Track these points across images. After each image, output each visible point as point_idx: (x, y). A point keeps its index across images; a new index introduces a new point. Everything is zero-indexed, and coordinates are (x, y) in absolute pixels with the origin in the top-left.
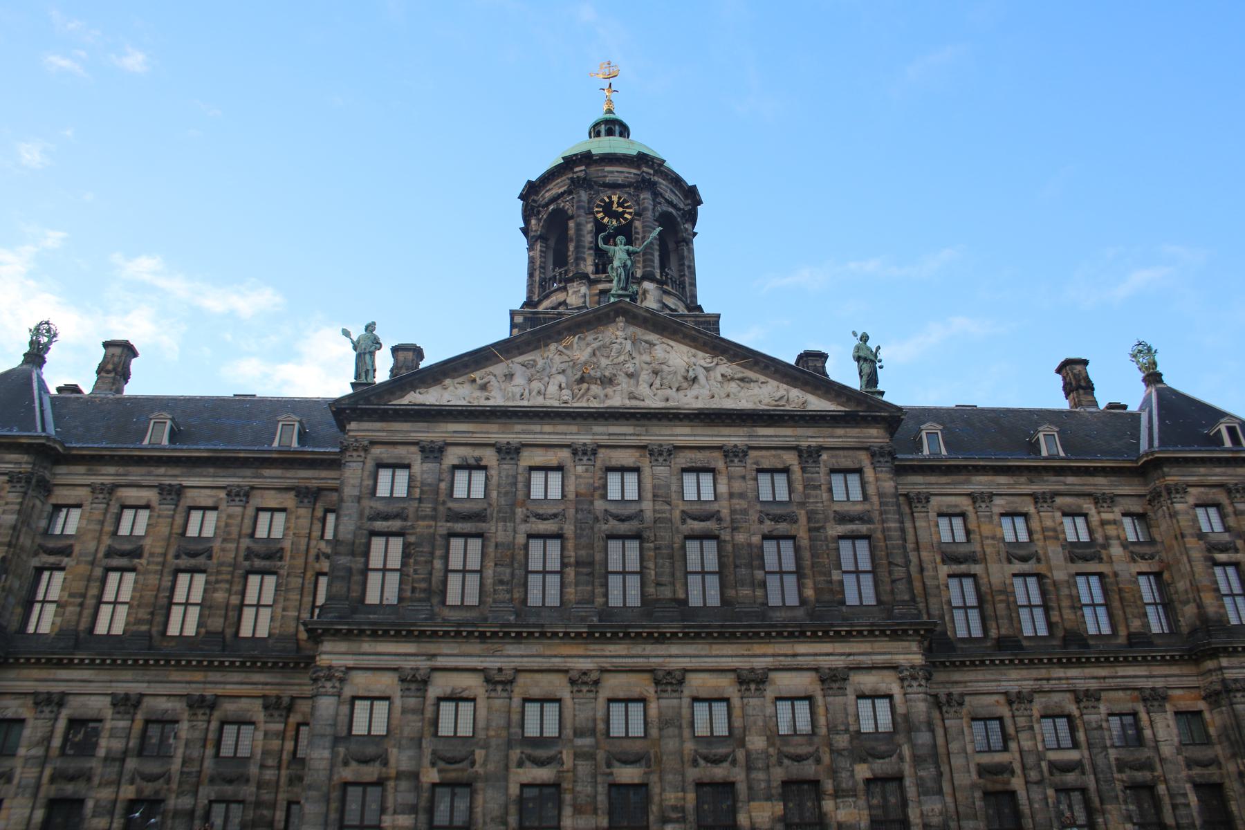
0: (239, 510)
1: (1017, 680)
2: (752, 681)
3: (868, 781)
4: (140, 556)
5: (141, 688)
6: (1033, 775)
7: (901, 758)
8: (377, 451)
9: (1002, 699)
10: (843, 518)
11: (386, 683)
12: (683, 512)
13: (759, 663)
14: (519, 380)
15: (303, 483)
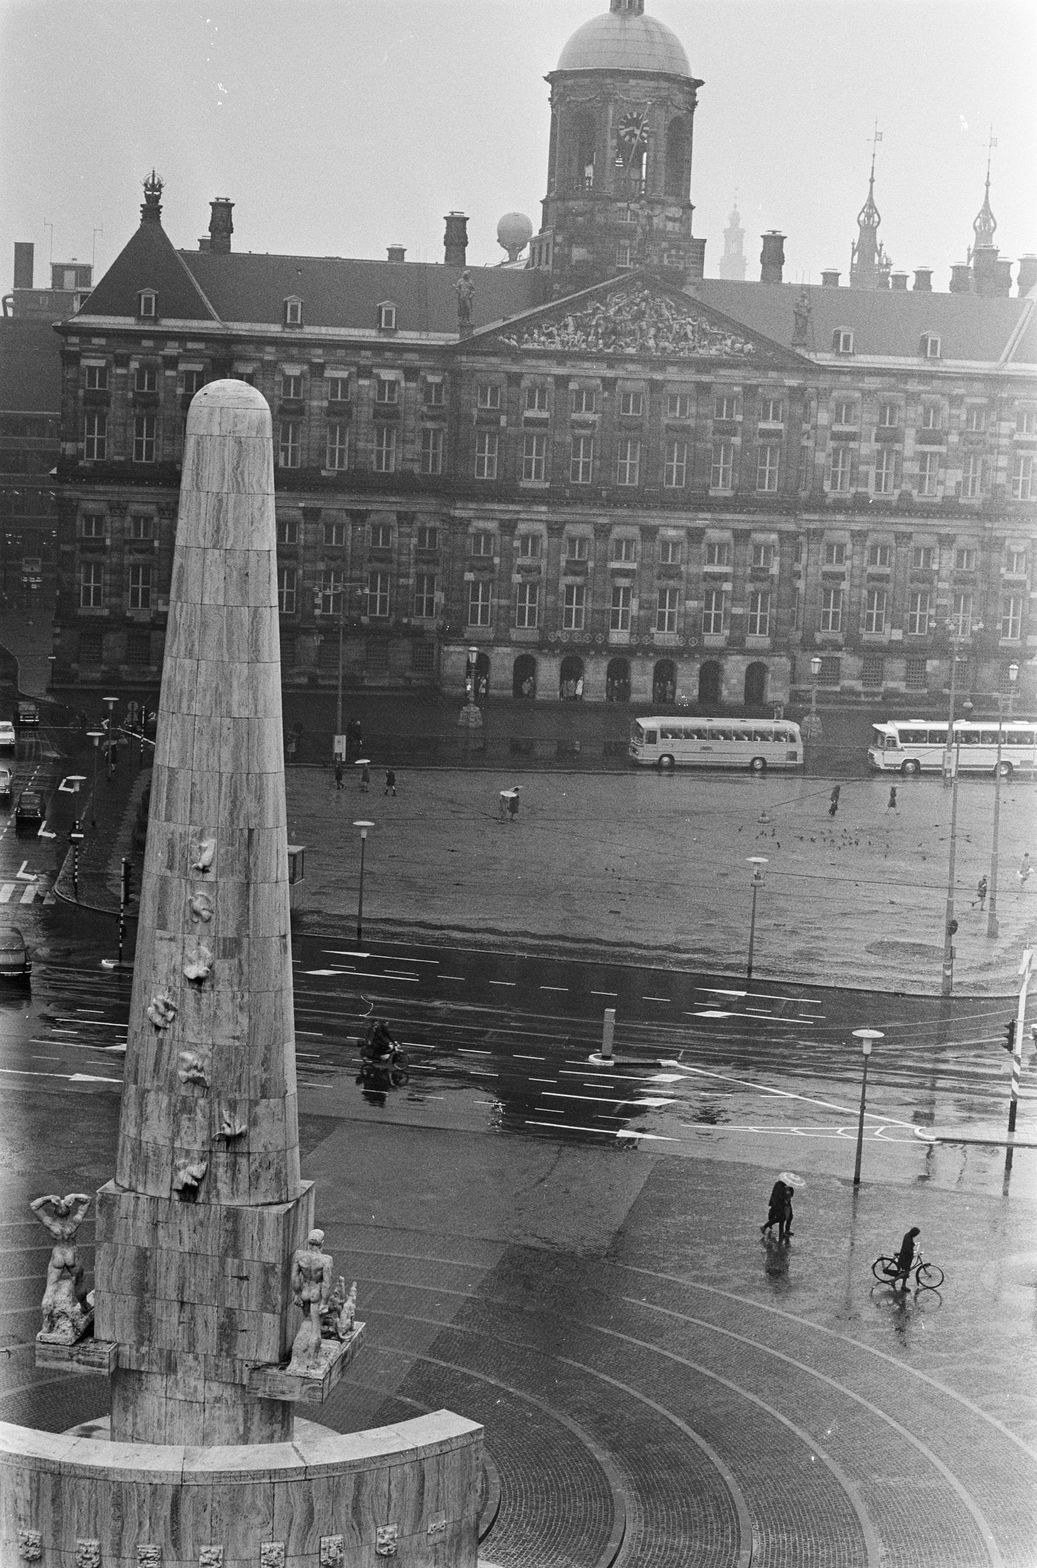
0: (363, 382)
1: (861, 522)
2: (695, 535)
3: (753, 593)
4: (303, 414)
5: (319, 504)
6: (857, 581)
7: (772, 582)
8: (478, 375)
9: (848, 534)
10: (766, 434)
11: (492, 526)
12: (667, 425)
13: (699, 523)
14: (571, 329)
15: (408, 365)
